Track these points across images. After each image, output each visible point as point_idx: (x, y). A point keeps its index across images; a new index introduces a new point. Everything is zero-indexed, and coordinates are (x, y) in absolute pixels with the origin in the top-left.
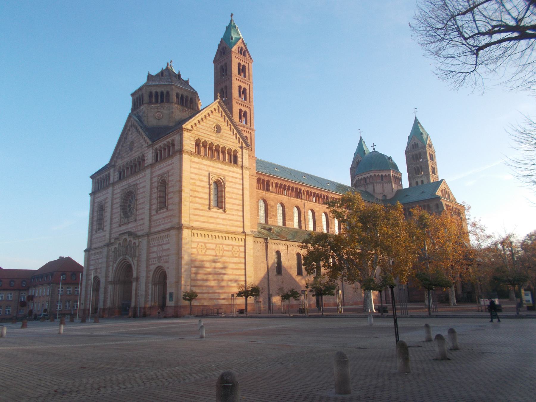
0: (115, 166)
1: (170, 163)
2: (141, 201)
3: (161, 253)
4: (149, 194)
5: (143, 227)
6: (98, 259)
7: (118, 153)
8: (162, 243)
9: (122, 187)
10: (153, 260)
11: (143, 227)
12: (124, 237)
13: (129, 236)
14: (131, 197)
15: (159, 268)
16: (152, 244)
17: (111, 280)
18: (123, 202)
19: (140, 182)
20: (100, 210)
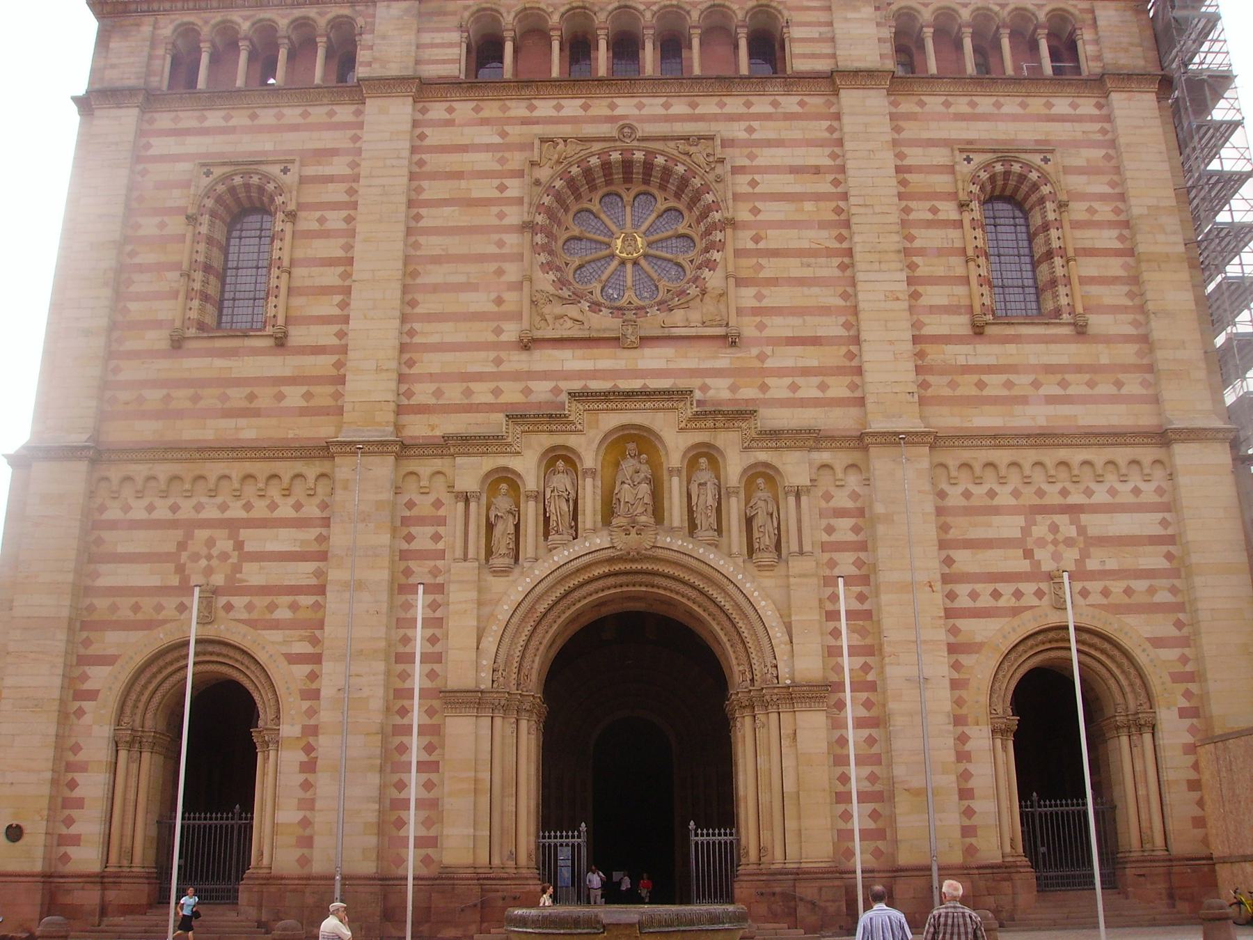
1: (1054, 111)
2: (775, 239)
3: (1070, 557)
4: (894, 218)
6: (232, 526)
8: (1076, 498)
9: (525, 122)
10: (985, 589)
11: (823, 387)
12: (612, 420)
13: (697, 416)
14: (596, 197)
15: (1051, 635)
16: (967, 494)
17: (469, 684)
19: (755, 136)
20: (213, 214)
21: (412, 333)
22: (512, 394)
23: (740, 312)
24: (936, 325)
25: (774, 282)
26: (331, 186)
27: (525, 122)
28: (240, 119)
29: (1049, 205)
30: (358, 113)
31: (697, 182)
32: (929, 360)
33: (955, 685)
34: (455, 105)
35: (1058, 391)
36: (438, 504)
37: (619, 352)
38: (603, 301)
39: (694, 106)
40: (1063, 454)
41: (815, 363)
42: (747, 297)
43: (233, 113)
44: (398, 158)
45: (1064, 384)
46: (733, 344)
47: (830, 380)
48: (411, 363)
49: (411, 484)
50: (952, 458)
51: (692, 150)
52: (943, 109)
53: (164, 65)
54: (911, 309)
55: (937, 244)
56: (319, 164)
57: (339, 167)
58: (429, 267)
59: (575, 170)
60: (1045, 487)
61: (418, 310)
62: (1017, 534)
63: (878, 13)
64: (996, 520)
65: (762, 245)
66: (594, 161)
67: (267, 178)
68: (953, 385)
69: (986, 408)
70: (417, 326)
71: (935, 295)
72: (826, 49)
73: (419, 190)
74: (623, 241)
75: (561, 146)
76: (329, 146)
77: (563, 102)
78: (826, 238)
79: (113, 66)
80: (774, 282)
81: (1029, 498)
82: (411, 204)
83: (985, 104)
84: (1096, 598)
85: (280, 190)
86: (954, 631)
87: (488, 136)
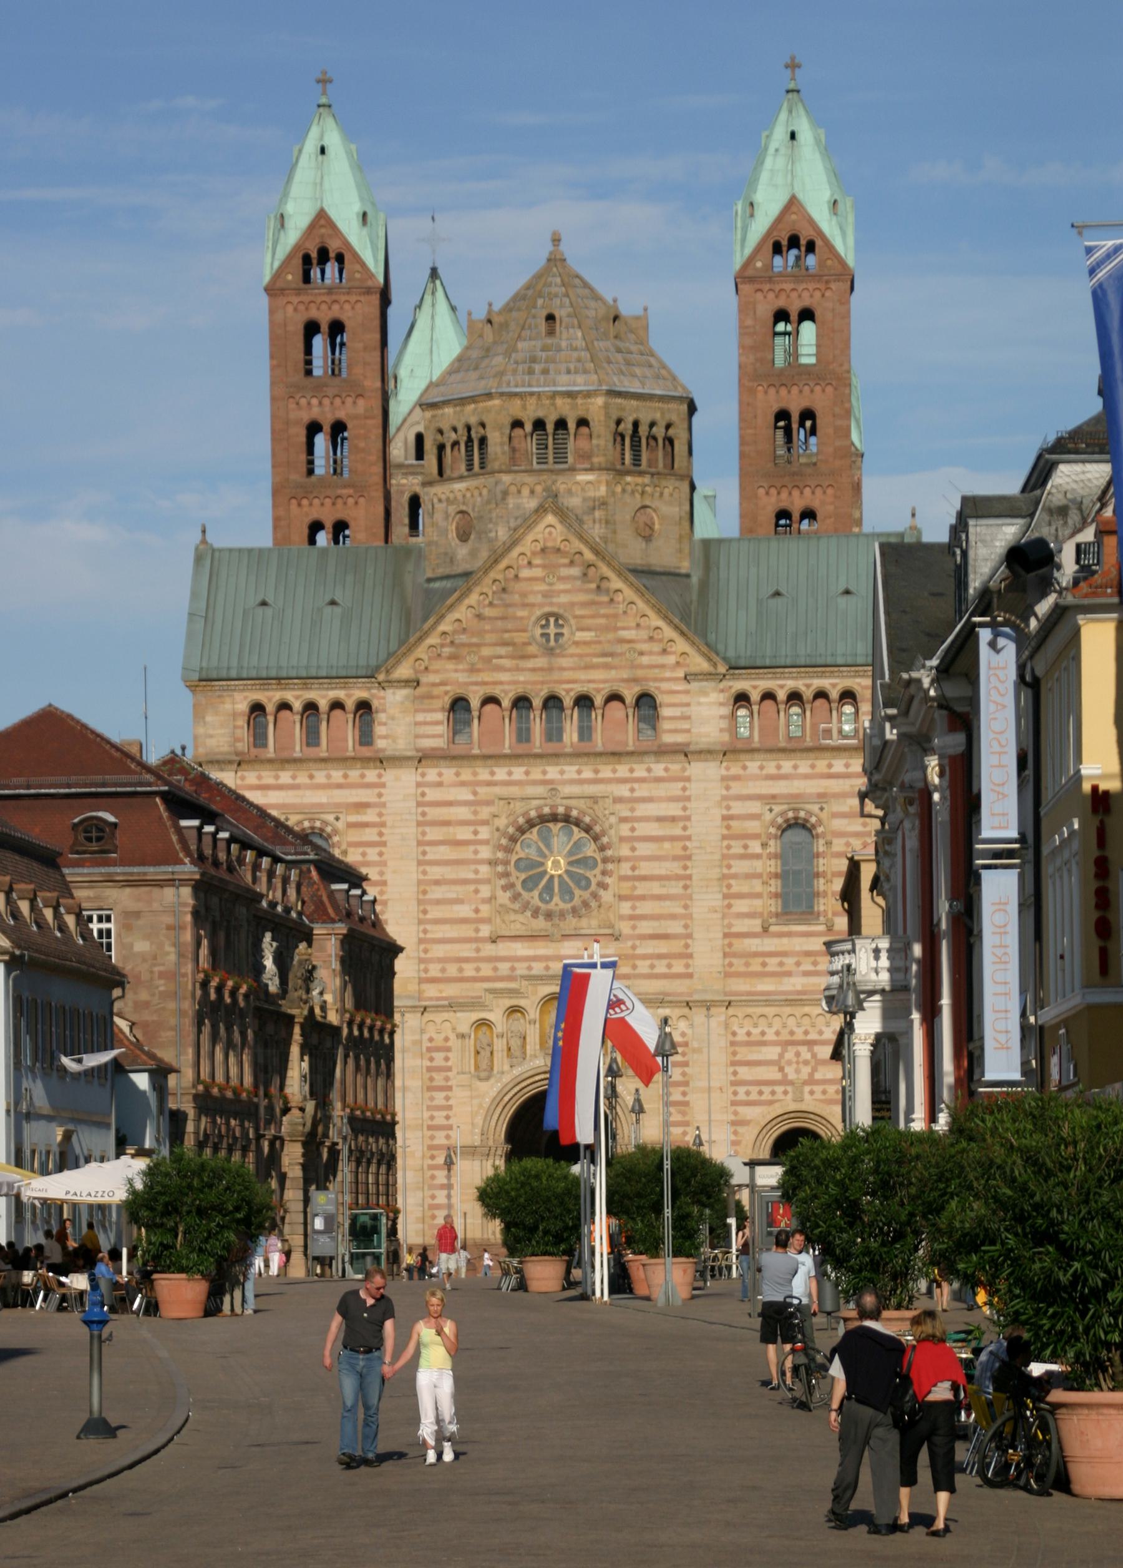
0: (418, 683)
1: (834, 770)
2: (645, 869)
3: (806, 1071)
4: (717, 857)
5: (669, 966)
7: (444, 633)
8: (813, 1036)
9: (489, 784)
10: (754, 1089)
11: (669, 966)
14: (535, 830)
15: (792, 1115)
16: (749, 1034)
17: (469, 1142)
18: (508, 850)
19: (637, 794)
21: (425, 931)
22: (486, 970)
23: (622, 918)
24: (740, 926)
25: (642, 898)
26: (367, 830)
27: (489, 784)
28: (302, 778)
29: (821, 842)
30: (380, 776)
31: (597, 829)
32: (734, 949)
33: (734, 1143)
34: (444, 771)
35: (810, 968)
36: (447, 1039)
37: (550, 944)
38: (540, 904)
39: (596, 772)
40: (807, 1009)
41: (664, 950)
42: (625, 908)
43: (298, 773)
44: (410, 813)
45: (815, 964)
46: (617, 939)
47: (674, 962)
48: (426, 951)
49: (431, 1026)
50: (741, 1012)
51: (596, 807)
52: (757, 771)
53: (243, 733)
54: (724, 917)
55: (746, 870)
56: (358, 813)
57: (370, 816)
58: (434, 887)
59: (521, 820)
60: (795, 1029)
61: (428, 916)
62: (776, 1057)
63: (722, 695)
64: (764, 1049)
65: (637, 873)
66: (533, 814)
67: (326, 823)
68: (747, 964)
69: (766, 980)
70: (428, 927)
71: (741, 906)
72: (685, 725)
73: (424, 834)
74: (553, 862)
75: (512, 806)
76: (364, 800)
77: (513, 769)
78: (675, 868)
79: (211, 736)
80: (642, 898)
81: (785, 1036)
82: (420, 843)
83: (787, 766)
84: (818, 1095)
85: (336, 832)
86: (736, 1113)
87: (465, 795)
